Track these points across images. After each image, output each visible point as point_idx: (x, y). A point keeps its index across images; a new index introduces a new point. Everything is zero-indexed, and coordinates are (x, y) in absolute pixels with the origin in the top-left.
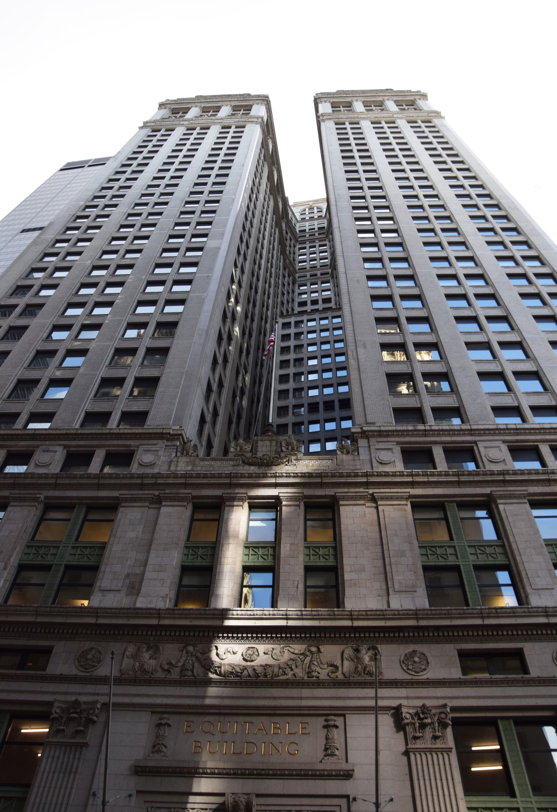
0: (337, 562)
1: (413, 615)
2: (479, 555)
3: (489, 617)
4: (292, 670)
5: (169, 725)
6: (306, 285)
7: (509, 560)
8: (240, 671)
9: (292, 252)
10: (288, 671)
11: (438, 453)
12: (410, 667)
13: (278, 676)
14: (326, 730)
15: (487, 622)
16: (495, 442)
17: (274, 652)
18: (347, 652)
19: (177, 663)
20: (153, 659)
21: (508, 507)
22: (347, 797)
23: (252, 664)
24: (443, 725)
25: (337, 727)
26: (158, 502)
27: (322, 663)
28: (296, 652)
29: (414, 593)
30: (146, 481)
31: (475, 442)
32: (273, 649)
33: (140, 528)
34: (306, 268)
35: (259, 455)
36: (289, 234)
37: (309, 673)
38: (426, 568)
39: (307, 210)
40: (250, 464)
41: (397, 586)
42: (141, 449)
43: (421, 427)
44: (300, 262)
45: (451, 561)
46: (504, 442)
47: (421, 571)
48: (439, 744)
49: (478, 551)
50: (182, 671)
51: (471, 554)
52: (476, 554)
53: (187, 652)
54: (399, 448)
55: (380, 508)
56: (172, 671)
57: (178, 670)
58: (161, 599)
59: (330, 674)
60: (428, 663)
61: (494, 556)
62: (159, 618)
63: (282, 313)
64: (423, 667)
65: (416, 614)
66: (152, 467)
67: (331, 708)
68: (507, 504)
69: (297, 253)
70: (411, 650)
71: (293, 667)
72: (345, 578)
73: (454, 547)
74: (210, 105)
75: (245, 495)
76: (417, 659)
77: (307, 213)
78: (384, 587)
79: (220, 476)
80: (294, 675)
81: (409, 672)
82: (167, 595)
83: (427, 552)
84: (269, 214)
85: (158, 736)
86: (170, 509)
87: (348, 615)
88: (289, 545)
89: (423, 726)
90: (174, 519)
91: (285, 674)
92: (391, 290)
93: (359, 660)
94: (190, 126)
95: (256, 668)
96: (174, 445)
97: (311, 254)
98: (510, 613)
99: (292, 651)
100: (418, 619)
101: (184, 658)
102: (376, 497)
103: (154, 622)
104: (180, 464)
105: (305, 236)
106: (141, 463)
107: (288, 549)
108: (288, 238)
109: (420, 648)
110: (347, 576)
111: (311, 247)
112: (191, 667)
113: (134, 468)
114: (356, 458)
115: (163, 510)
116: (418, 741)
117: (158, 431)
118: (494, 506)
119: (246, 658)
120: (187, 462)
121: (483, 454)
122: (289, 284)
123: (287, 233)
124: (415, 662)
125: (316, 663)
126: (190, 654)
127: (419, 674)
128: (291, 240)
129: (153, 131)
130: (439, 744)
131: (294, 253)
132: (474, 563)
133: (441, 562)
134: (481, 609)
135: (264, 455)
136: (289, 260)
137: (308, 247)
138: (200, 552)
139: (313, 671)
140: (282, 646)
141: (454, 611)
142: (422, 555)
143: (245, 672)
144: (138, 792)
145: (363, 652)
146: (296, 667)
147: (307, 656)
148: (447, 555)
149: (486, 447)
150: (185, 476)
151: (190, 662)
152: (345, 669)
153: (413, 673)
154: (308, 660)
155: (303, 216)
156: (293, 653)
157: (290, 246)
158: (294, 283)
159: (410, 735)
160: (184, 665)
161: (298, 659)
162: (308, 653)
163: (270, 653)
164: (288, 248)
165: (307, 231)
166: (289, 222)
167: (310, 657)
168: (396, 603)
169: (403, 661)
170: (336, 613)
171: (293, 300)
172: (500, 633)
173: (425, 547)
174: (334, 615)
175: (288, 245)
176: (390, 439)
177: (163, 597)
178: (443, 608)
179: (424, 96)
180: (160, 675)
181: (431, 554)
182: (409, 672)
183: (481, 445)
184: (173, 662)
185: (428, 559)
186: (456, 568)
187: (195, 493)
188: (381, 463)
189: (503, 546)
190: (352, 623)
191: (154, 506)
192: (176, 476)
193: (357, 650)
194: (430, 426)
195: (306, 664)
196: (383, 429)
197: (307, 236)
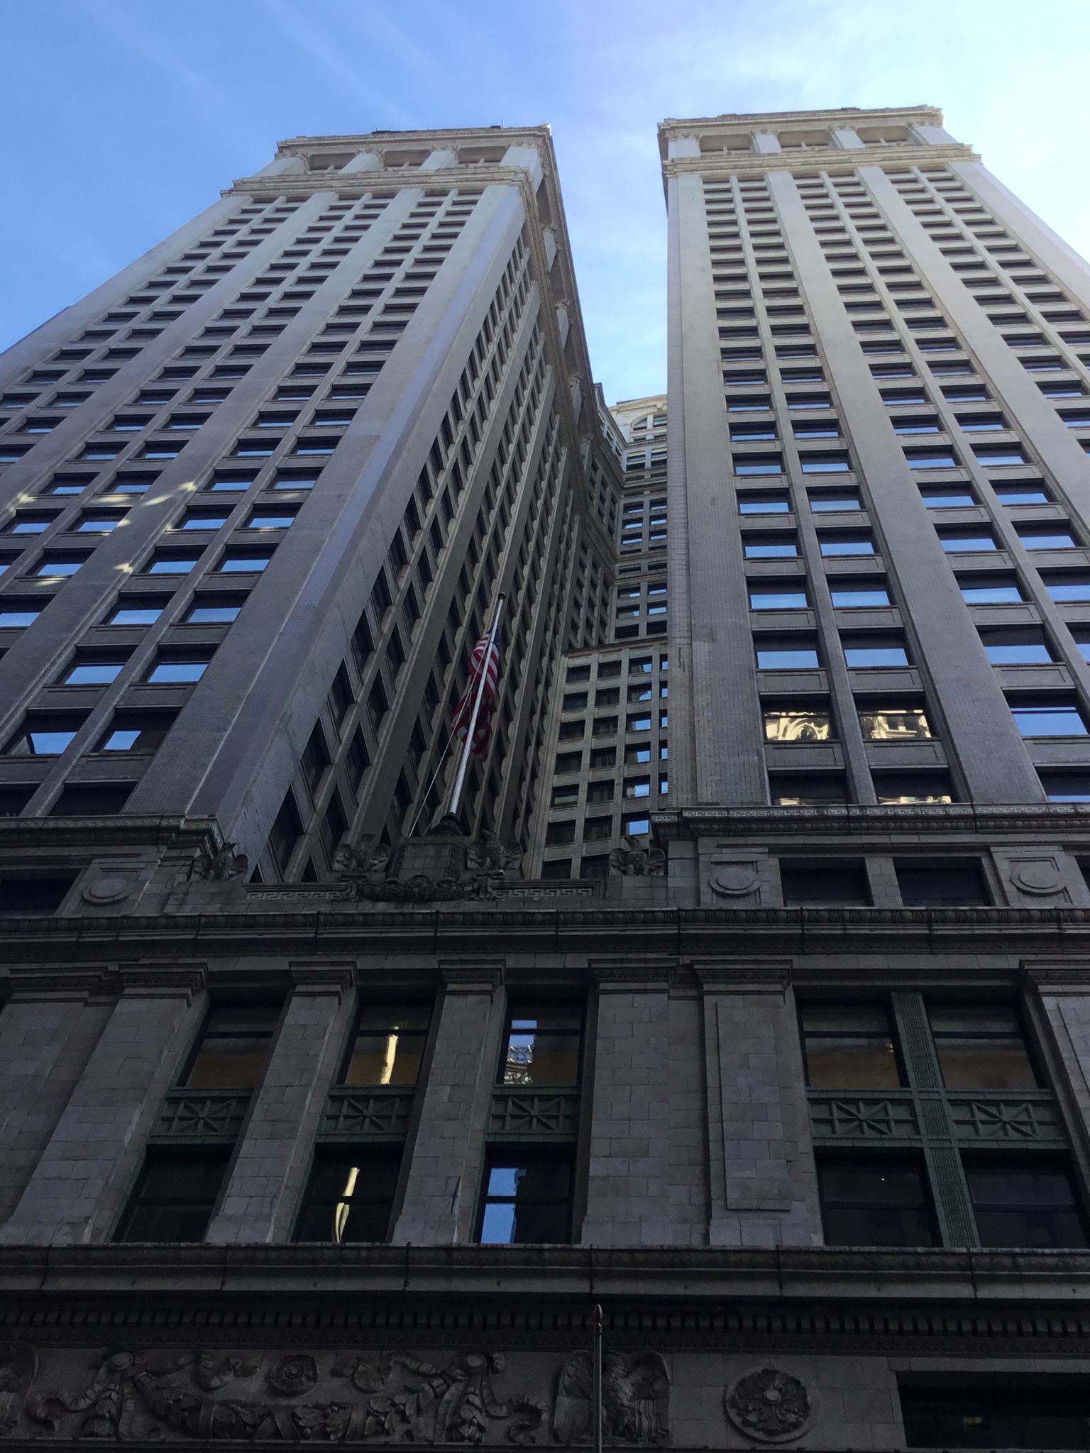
2: (979, 1124)
3: (993, 1280)
4: (404, 1419)
6: (637, 590)
7: (1068, 1140)
8: (251, 1422)
9: (606, 513)
10: (391, 1421)
11: (881, 872)
12: (752, 1418)
13: (363, 1437)
15: (987, 1292)
16: (1041, 848)
17: (361, 1368)
18: (571, 1370)
19: (76, 1401)
20: (9, 1391)
21: (1068, 1004)
23: (293, 1402)
26: (112, 989)
27: (494, 1402)
28: (425, 1368)
29: (783, 1216)
30: (89, 938)
31: (986, 848)
32: (359, 1360)
34: (640, 550)
35: (405, 876)
36: (601, 472)
37: (454, 1427)
38: (826, 1158)
39: (650, 419)
40: (375, 898)
41: (733, 1196)
42: (95, 866)
43: (837, 811)
44: (625, 538)
45: (899, 1137)
46: (1067, 847)
47: (809, 1163)
49: (979, 1116)
50: (85, 1422)
51: (958, 1122)
52: (973, 1123)
53: (111, 1371)
54: (774, 862)
55: (708, 1000)
56: (56, 1424)
58: (66, 1229)
59: (513, 1433)
60: (806, 1407)
61: (1027, 1129)
62: (45, 1274)
63: (571, 646)
64: (792, 1418)
65: (778, 1262)
66: (116, 906)
68: (1065, 994)
69: (621, 516)
70: (759, 1369)
72: (591, 1173)
73: (910, 1103)
74: (403, 151)
75: (351, 968)
76: (772, 1395)
77: (650, 426)
78: (699, 1199)
79: (289, 922)
82: (87, 1218)
83: (831, 1114)
84: (541, 406)
86: (142, 1005)
88: (448, 1088)
90: (154, 1030)
91: (381, 1430)
92: (797, 519)
94: (349, 190)
95: (299, 1411)
96: (187, 858)
97: (653, 518)
98: (1056, 1268)
99: (414, 1365)
100: (781, 1279)
101: (98, 1388)
102: (700, 973)
103: (30, 1284)
104: (190, 898)
105: (643, 477)
106: (87, 897)
107: (446, 1098)
108: (598, 481)
109: (784, 1364)
110: (597, 1168)
111: (653, 503)
112: (114, 1411)
113: (69, 908)
114: (659, 883)
115: (124, 1006)
117: (148, 823)
118: (1029, 1002)
119: (277, 1385)
120: (212, 893)
121: (1004, 876)
122: (593, 585)
123: (595, 468)
124: (768, 1403)
125: (477, 1401)
126: (118, 1376)
127: (777, 1439)
128: (604, 485)
129: (255, 202)
131: (612, 516)
132: (965, 1145)
133: (870, 1140)
134: (969, 1254)
135: (417, 876)
136: (598, 531)
137: (646, 505)
138: (206, 1111)
139: (463, 1422)
140: (385, 1353)
141: (889, 1258)
142: (816, 1121)
143: (267, 1422)
145: (619, 1370)
146: (419, 1411)
147: (455, 1380)
148: (887, 1122)
149: (1013, 860)
150: (195, 923)
151: (114, 1396)
152: (560, 1419)
154: (455, 1390)
155: (640, 434)
156: (416, 1373)
157: (602, 499)
158: (607, 585)
160: (94, 1404)
161: (427, 1387)
162: (457, 1373)
164: (596, 501)
165: (648, 465)
166: (601, 444)
167: (461, 1387)
168: (725, 1235)
169: (733, 1399)
171: (603, 624)
172: (1028, 1328)
173: (827, 1102)
175: (596, 495)
176: (750, 840)
177: (72, 1225)
178: (855, 1249)
179: (931, 116)
181: (841, 1121)
183: (1000, 855)
184: (66, 1397)
185: (834, 1131)
186: (913, 1160)
187: (215, 965)
188: (718, 894)
189: (1053, 1104)
190: (592, 1288)
191: (102, 999)
192: (171, 923)
194: (862, 808)
195: (449, 1402)
196: (734, 814)
197: (647, 476)
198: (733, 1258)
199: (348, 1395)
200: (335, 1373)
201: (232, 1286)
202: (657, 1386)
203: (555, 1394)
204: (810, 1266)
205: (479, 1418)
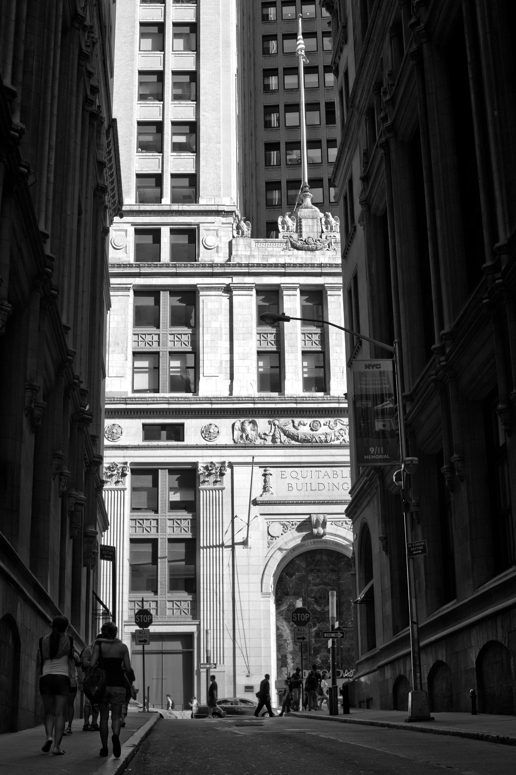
4: (342, 436)
5: (271, 475)
10: (340, 437)
57: (271, 438)
71: (344, 434)
80: (344, 440)
99: (342, 423)
103: (251, 406)
143: (314, 439)
144: (261, 514)
146: (345, 434)
160: (274, 435)
163: (328, 424)
184: (267, 433)
200: (324, 425)
201: (299, 406)
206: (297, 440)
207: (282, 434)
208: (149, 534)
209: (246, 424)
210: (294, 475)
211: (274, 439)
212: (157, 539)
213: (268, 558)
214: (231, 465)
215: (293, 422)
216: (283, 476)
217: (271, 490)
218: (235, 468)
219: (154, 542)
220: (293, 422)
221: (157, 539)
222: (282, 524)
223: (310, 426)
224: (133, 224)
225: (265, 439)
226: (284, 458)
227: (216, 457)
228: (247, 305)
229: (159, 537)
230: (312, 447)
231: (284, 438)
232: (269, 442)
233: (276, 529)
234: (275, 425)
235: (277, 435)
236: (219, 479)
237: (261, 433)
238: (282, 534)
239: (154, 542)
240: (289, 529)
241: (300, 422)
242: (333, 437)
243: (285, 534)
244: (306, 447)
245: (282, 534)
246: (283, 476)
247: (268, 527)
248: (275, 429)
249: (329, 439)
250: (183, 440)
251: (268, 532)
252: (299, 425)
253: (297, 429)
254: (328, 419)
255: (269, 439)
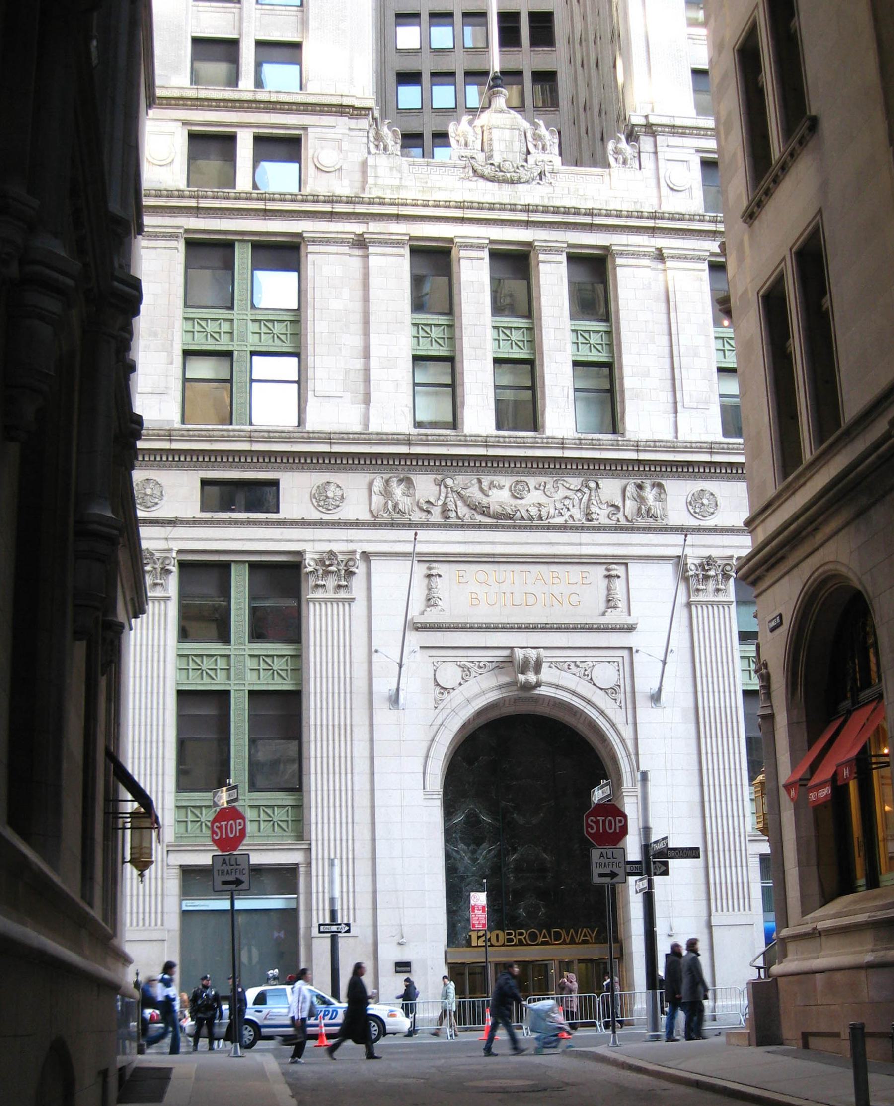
0: (613, 357)
1: (707, 448)
4: (568, 509)
5: (440, 576)
10: (564, 511)
12: (698, 510)
14: (607, 580)
22: (630, 649)
24: (726, 576)
25: (619, 577)
29: (707, 412)
33: (346, 293)
48: (721, 598)
60: (717, 505)
64: (712, 510)
67: (614, 557)
71: (570, 507)
76: (705, 501)
78: (671, 400)
80: (571, 516)
81: (696, 515)
85: (430, 589)
87: (633, 446)
89: (706, 578)
93: (642, 500)
99: (567, 486)
116: (701, 593)
124: (703, 504)
125: (595, 502)
130: (721, 598)
144: (421, 647)
153: (700, 517)
159: (693, 587)
160: (445, 504)
162: (586, 490)
163: (542, 488)
169: (690, 502)
170: (620, 443)
174: (618, 445)
180: (418, 516)
182: (696, 515)
184: (432, 500)
193: (640, 487)
198: (694, 445)
199: (543, 499)
200: (536, 488)
202: (662, 496)
203: (624, 500)
204: (723, 449)
205: (598, 511)
206: (489, 516)
207: (459, 503)
208: (213, 682)
209: (394, 483)
210: (482, 577)
211: (445, 511)
212: (228, 692)
213: (435, 728)
214: (366, 556)
215: (480, 481)
216: (461, 579)
217: (440, 603)
218: (375, 564)
219: (223, 696)
220: (480, 481)
221: (228, 692)
222: (460, 666)
223: (511, 490)
224: (185, 123)
225: (429, 512)
226: (463, 546)
227: (337, 542)
228: (393, 272)
229: (232, 688)
230: (514, 528)
231: (463, 510)
232: (436, 517)
233: (450, 675)
234: (446, 486)
235: (451, 506)
236: (343, 583)
237: (421, 501)
238: (460, 684)
239: (223, 696)
240: (473, 674)
241: (492, 483)
242: (552, 511)
243: (466, 685)
244: (503, 527)
245: (460, 684)
246: (461, 579)
247: (435, 671)
248: (447, 493)
249: (544, 513)
250: (278, 512)
251: (435, 679)
252: (490, 489)
253: (488, 496)
254: (542, 479)
255: (436, 511)
